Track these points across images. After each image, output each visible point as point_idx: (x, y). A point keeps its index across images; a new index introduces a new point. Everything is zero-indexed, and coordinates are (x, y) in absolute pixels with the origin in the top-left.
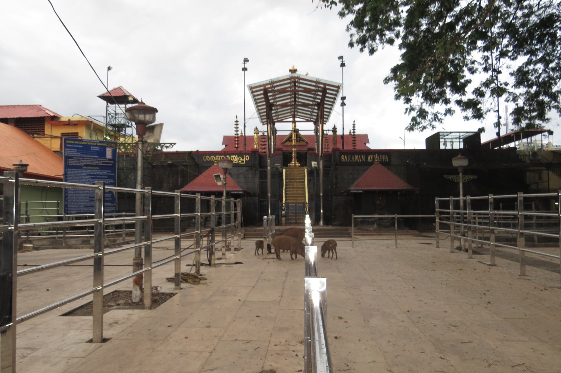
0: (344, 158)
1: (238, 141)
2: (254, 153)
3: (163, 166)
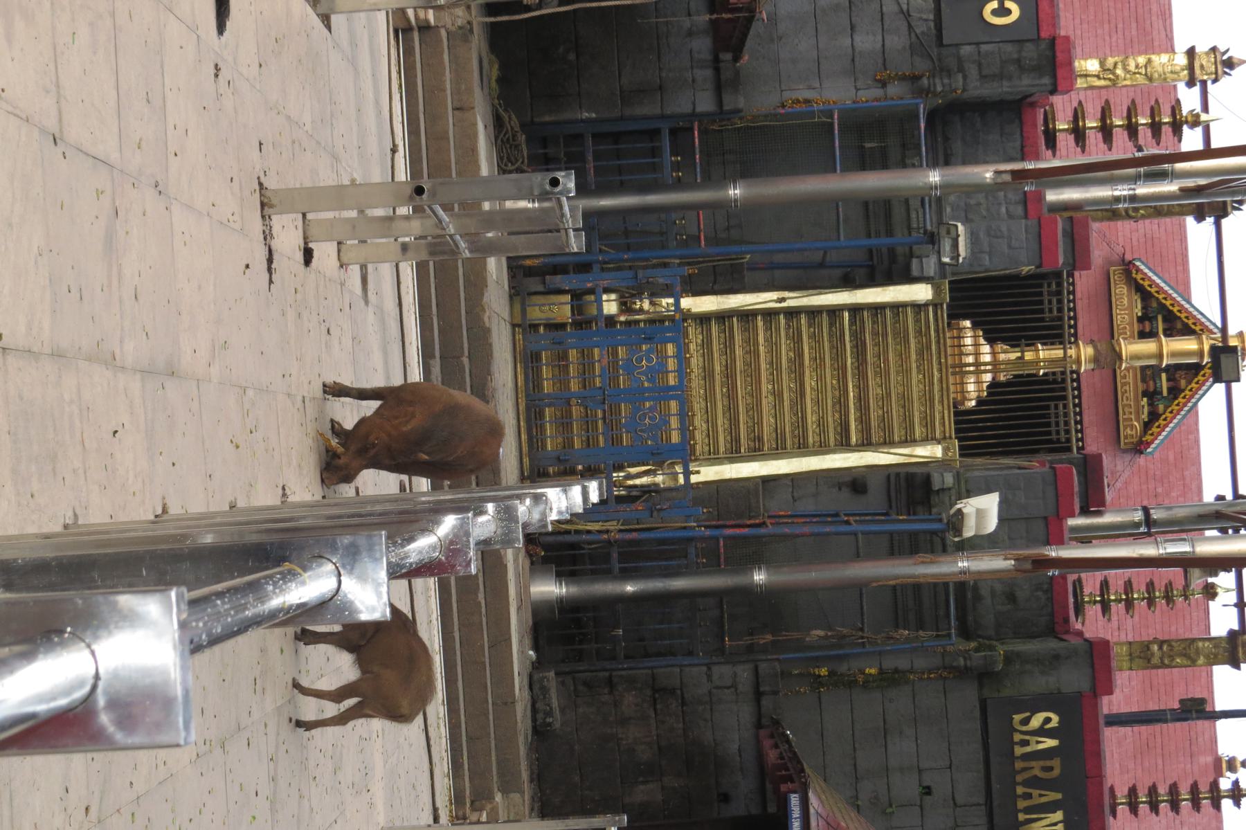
0: (1038, 730)
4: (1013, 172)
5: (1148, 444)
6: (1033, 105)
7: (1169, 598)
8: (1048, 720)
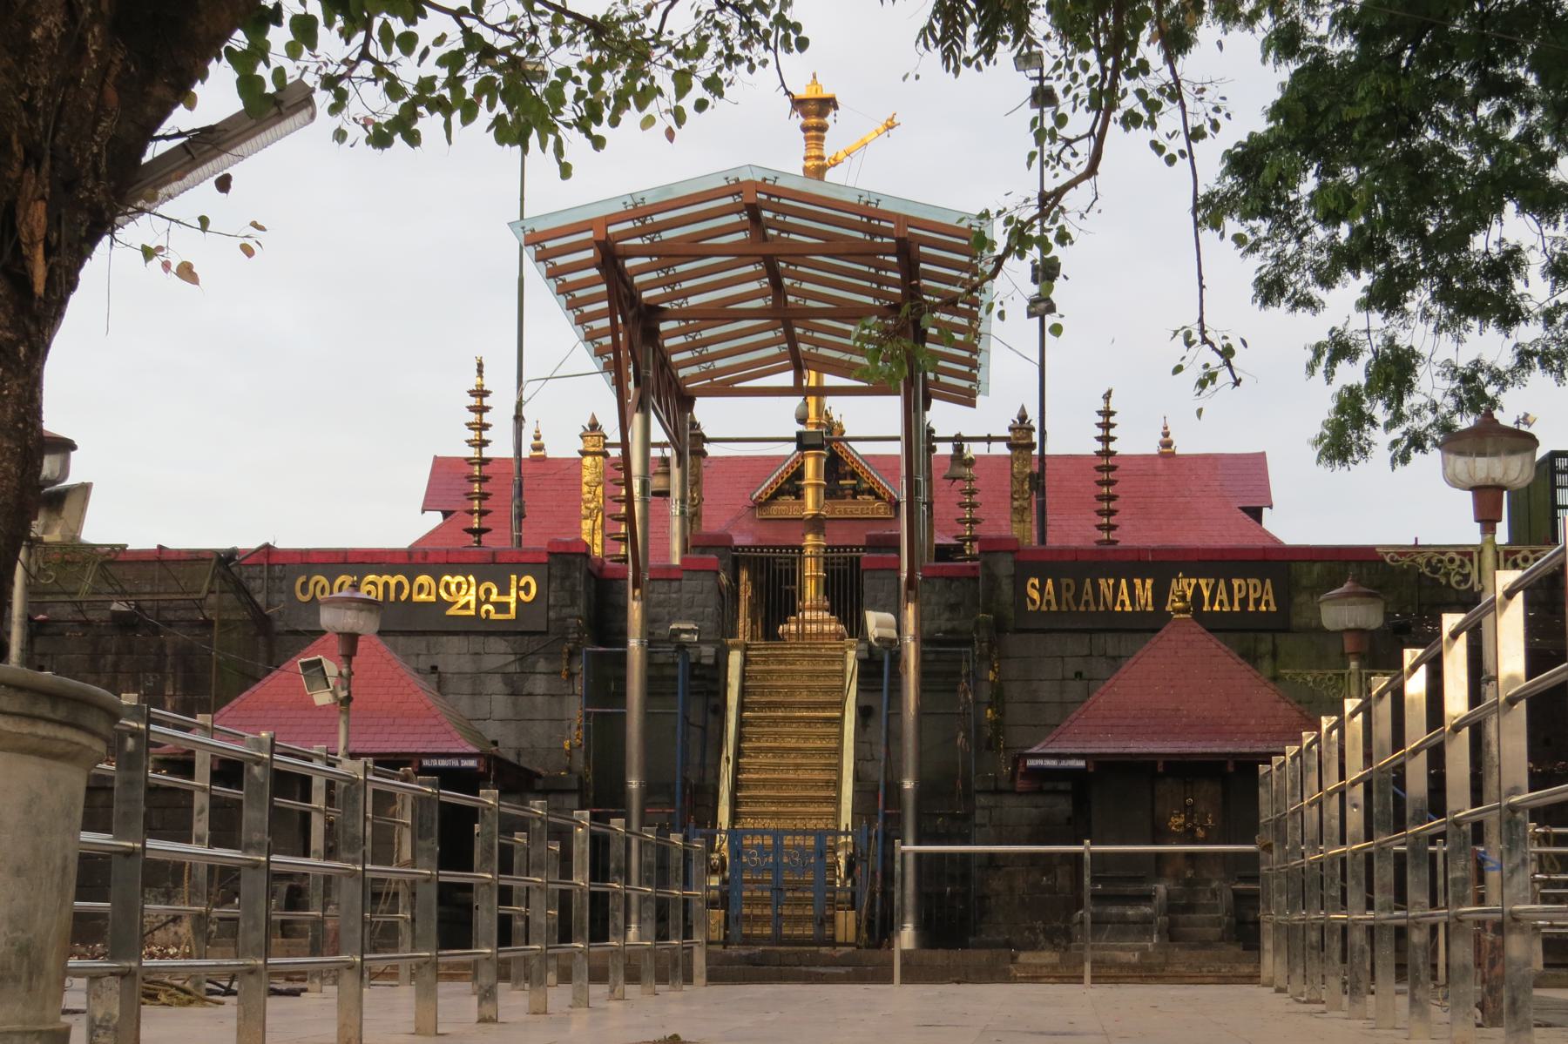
1: (484, 496)
2: (565, 564)
3: (87, 624)
4: (635, 587)
5: (891, 497)
6: (601, 570)
7: (972, 493)
8: (1033, 586)
